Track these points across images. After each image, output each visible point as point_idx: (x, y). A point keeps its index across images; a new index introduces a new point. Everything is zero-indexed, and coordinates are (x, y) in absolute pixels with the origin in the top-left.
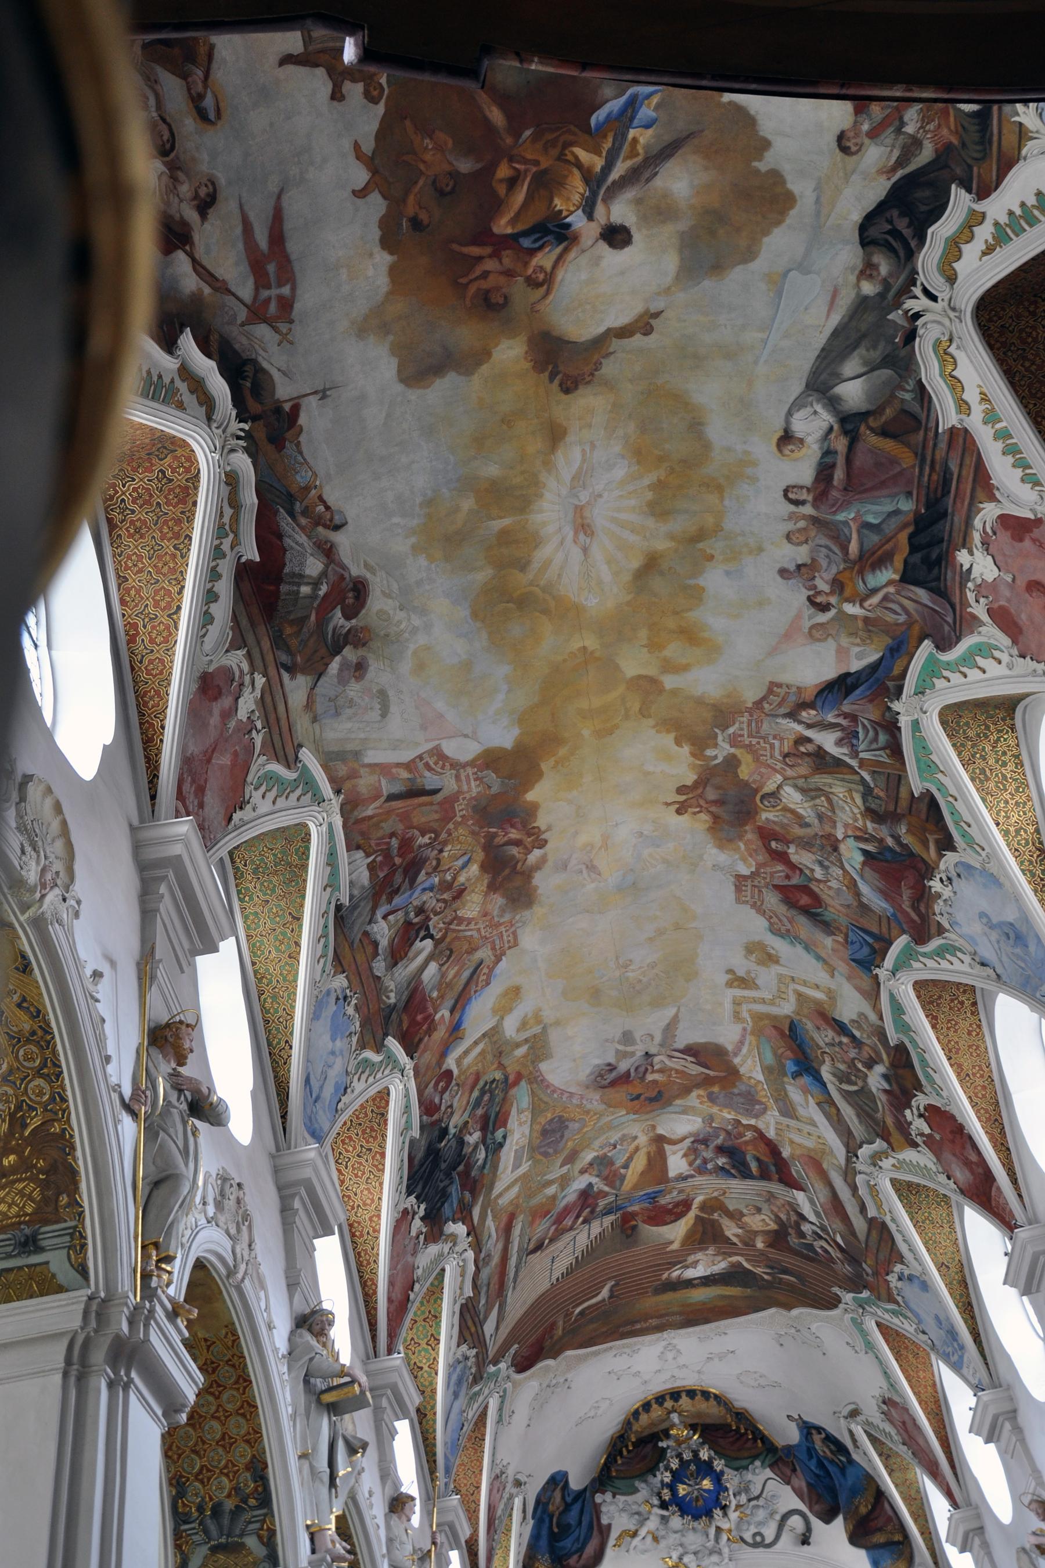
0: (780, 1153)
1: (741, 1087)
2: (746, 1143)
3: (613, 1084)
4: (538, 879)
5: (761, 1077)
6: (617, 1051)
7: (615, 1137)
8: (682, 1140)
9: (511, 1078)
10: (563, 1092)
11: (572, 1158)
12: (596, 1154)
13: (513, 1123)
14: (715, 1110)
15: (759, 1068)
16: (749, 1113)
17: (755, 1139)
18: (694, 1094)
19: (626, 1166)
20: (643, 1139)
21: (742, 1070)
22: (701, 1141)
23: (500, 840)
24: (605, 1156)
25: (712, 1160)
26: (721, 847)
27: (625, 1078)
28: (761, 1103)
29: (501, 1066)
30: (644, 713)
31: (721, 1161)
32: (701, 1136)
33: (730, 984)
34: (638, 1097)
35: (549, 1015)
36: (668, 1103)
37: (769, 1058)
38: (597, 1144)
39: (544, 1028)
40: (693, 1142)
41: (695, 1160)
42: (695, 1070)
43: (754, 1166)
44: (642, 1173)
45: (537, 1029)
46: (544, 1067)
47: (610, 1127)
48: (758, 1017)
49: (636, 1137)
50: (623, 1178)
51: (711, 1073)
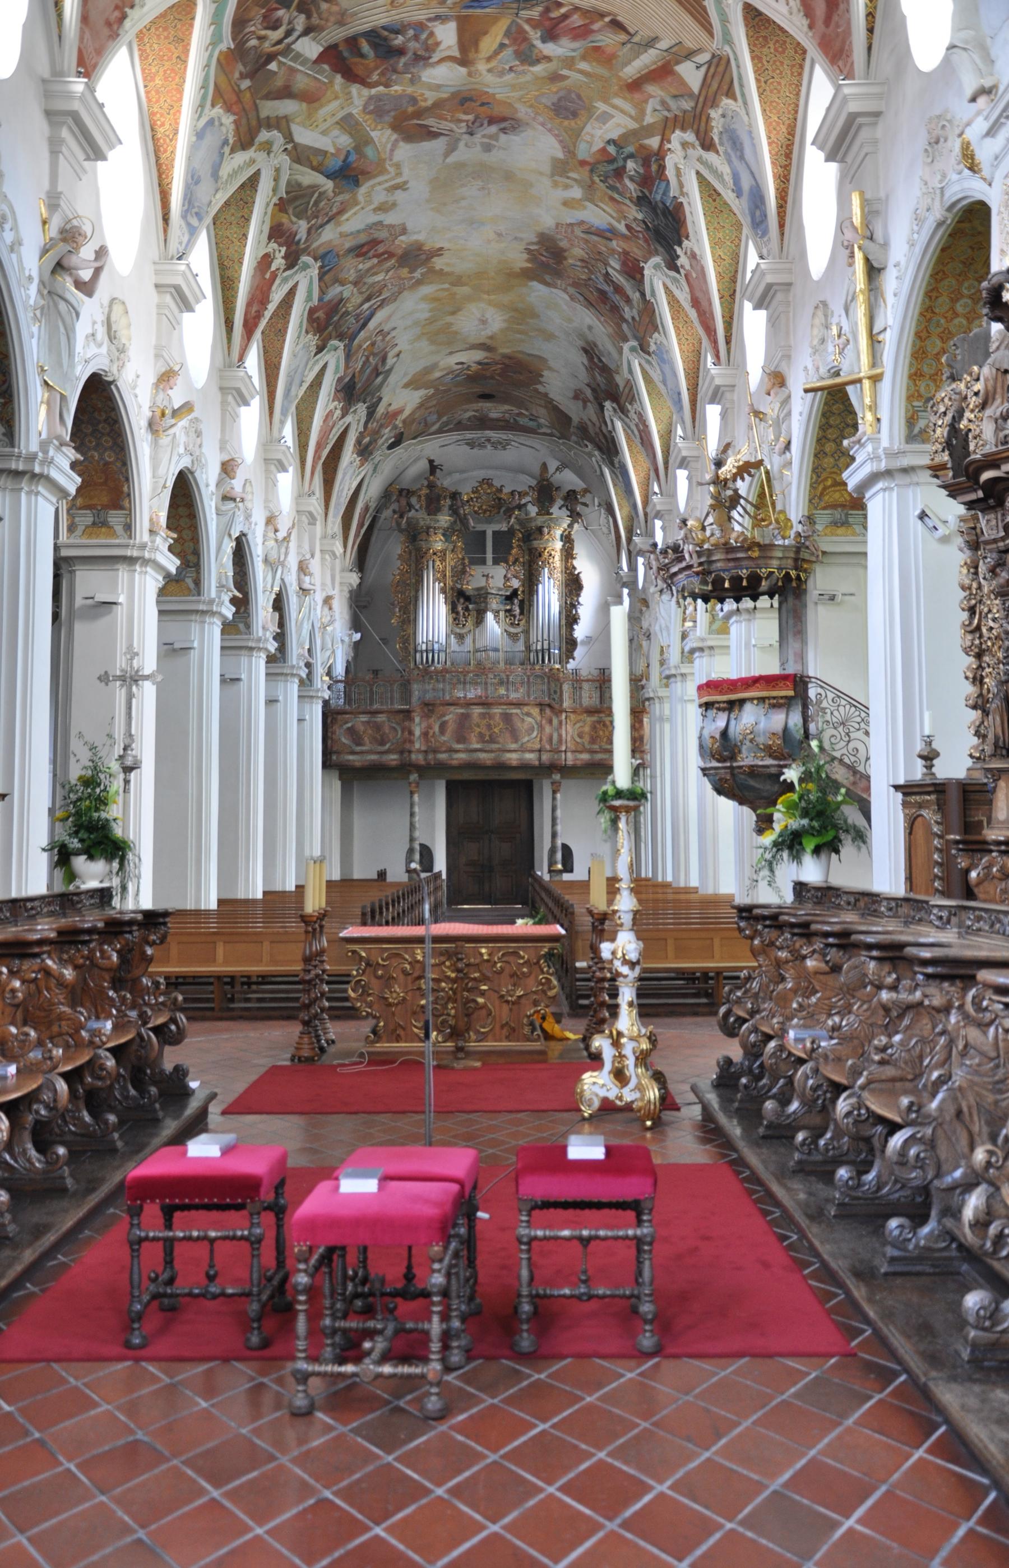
0: (343, 77)
1: (388, 119)
2: (376, 68)
3: (504, 119)
4: (535, 240)
5: (373, 134)
6: (497, 140)
7: (509, 77)
8: (442, 60)
9: (588, 168)
10: (550, 130)
11: (555, 78)
12: (532, 69)
13: (598, 145)
14: (410, 90)
15: (376, 139)
16: (378, 98)
17: (368, 76)
18: (429, 103)
19: (502, 46)
20: (482, 67)
21: (389, 131)
22: (422, 59)
23: (551, 261)
24: (523, 62)
25: (409, 40)
26: (417, 241)
27: (492, 121)
28: (370, 113)
29: (593, 182)
30: (460, 277)
31: (399, 40)
32: (421, 63)
33: (406, 183)
34: (483, 104)
35: (547, 182)
36: (454, 95)
37: (369, 151)
38: (528, 77)
39: (553, 175)
40: (430, 58)
41: (427, 39)
42: (430, 122)
43: (365, 47)
44: (485, 33)
45: (556, 178)
46: (560, 155)
47: (513, 87)
48: (383, 171)
49: (489, 71)
50: (507, 34)
51: (416, 121)
